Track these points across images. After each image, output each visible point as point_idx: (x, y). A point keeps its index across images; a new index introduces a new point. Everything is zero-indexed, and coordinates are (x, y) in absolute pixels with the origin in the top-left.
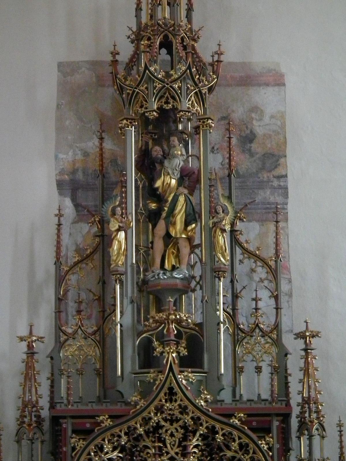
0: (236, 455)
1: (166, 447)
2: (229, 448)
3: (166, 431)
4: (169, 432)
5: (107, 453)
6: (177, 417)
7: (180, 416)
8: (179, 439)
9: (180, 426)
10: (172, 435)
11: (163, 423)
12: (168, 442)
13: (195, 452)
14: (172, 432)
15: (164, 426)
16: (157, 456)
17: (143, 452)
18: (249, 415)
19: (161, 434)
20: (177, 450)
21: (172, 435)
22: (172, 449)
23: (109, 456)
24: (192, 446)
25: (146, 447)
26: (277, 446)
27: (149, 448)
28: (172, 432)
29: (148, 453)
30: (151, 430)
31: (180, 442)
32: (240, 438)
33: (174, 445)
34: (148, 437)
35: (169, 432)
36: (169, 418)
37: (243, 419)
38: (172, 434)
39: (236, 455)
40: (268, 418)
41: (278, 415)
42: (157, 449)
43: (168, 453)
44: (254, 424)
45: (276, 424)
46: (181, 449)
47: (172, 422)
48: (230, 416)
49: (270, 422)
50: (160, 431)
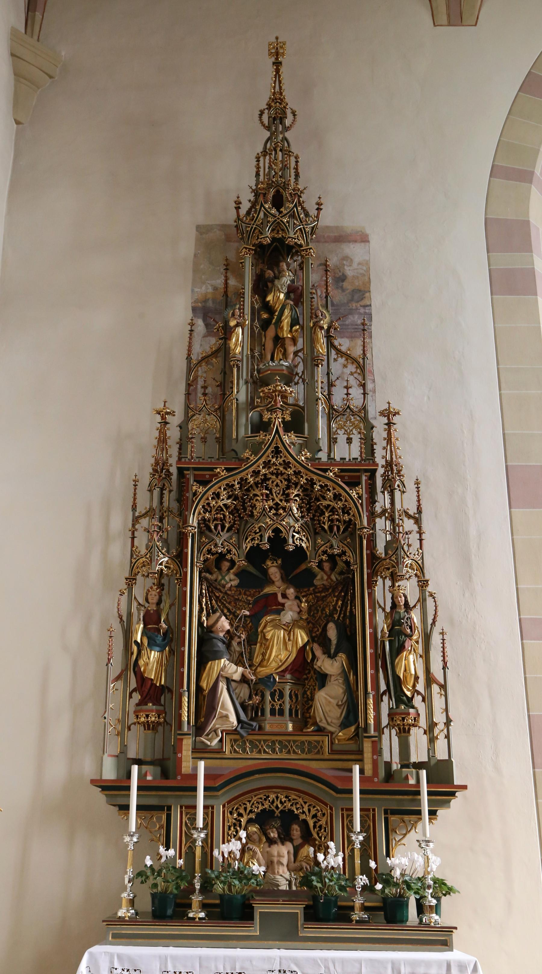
0: (331, 503)
1: (272, 495)
2: (324, 498)
3: (273, 482)
4: (275, 483)
5: (223, 500)
6: (281, 471)
7: (284, 471)
8: (283, 489)
9: (284, 479)
10: (277, 485)
11: (269, 476)
12: (274, 491)
13: (296, 500)
14: (277, 483)
15: (270, 478)
16: (264, 501)
17: (253, 500)
18: (342, 471)
19: (268, 484)
20: (282, 498)
21: (277, 485)
22: (277, 496)
23: (225, 502)
24: (294, 495)
25: (255, 495)
26: (365, 496)
27: (258, 496)
28: (277, 483)
29: (257, 500)
30: (260, 481)
31: (284, 491)
32: (334, 489)
33: (279, 494)
34: (257, 487)
35: (275, 483)
36: (275, 471)
37: (337, 473)
38: (277, 485)
39: (331, 503)
40: (358, 474)
41: (366, 471)
42: (265, 496)
43: (273, 500)
44: (346, 478)
45: (364, 478)
46: (285, 496)
47: (277, 475)
48: (325, 471)
49: (359, 478)
50: (268, 483)
